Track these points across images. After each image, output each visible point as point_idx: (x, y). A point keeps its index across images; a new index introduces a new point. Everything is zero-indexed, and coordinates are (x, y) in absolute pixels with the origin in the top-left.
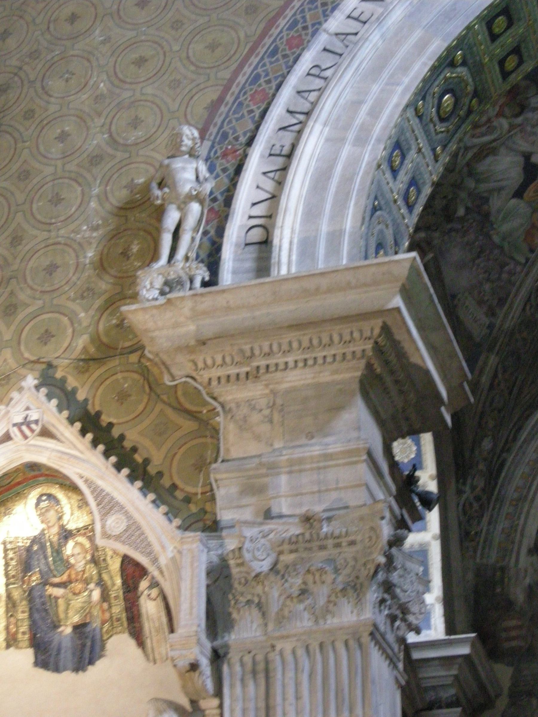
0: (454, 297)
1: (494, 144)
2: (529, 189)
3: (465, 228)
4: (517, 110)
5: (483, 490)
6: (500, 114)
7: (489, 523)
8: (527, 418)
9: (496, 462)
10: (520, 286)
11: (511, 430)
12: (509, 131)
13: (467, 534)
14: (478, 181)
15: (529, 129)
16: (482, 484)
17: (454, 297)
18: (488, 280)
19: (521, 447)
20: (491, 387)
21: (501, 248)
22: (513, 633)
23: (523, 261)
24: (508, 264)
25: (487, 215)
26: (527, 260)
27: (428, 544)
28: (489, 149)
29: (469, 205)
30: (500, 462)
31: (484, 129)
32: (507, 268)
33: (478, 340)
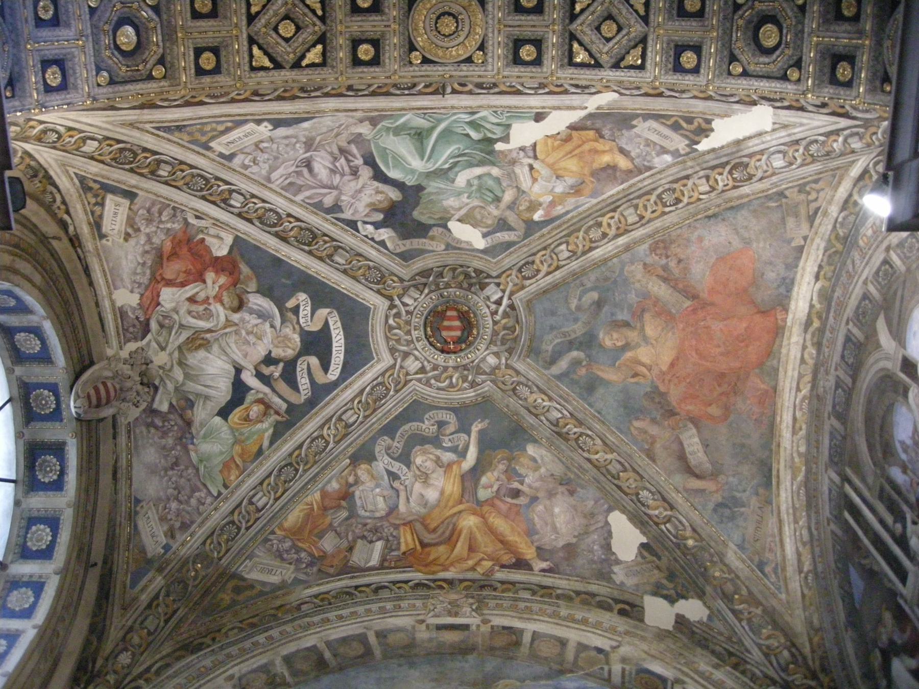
1: (208, 336)
2: (234, 412)
3: (165, 429)
4: (236, 303)
6: (218, 299)
8: (178, 659)
9: (131, 681)
10: (207, 518)
11: (156, 662)
12: (225, 328)
14: (187, 376)
15: (244, 333)
17: (138, 501)
18: (177, 499)
19: (163, 680)
20: (149, 606)
21: (197, 470)
23: (216, 494)
24: (199, 490)
25: (189, 424)
26: (220, 494)
28: (203, 339)
29: (174, 403)
31: (201, 308)
32: (197, 494)
33: (149, 555)
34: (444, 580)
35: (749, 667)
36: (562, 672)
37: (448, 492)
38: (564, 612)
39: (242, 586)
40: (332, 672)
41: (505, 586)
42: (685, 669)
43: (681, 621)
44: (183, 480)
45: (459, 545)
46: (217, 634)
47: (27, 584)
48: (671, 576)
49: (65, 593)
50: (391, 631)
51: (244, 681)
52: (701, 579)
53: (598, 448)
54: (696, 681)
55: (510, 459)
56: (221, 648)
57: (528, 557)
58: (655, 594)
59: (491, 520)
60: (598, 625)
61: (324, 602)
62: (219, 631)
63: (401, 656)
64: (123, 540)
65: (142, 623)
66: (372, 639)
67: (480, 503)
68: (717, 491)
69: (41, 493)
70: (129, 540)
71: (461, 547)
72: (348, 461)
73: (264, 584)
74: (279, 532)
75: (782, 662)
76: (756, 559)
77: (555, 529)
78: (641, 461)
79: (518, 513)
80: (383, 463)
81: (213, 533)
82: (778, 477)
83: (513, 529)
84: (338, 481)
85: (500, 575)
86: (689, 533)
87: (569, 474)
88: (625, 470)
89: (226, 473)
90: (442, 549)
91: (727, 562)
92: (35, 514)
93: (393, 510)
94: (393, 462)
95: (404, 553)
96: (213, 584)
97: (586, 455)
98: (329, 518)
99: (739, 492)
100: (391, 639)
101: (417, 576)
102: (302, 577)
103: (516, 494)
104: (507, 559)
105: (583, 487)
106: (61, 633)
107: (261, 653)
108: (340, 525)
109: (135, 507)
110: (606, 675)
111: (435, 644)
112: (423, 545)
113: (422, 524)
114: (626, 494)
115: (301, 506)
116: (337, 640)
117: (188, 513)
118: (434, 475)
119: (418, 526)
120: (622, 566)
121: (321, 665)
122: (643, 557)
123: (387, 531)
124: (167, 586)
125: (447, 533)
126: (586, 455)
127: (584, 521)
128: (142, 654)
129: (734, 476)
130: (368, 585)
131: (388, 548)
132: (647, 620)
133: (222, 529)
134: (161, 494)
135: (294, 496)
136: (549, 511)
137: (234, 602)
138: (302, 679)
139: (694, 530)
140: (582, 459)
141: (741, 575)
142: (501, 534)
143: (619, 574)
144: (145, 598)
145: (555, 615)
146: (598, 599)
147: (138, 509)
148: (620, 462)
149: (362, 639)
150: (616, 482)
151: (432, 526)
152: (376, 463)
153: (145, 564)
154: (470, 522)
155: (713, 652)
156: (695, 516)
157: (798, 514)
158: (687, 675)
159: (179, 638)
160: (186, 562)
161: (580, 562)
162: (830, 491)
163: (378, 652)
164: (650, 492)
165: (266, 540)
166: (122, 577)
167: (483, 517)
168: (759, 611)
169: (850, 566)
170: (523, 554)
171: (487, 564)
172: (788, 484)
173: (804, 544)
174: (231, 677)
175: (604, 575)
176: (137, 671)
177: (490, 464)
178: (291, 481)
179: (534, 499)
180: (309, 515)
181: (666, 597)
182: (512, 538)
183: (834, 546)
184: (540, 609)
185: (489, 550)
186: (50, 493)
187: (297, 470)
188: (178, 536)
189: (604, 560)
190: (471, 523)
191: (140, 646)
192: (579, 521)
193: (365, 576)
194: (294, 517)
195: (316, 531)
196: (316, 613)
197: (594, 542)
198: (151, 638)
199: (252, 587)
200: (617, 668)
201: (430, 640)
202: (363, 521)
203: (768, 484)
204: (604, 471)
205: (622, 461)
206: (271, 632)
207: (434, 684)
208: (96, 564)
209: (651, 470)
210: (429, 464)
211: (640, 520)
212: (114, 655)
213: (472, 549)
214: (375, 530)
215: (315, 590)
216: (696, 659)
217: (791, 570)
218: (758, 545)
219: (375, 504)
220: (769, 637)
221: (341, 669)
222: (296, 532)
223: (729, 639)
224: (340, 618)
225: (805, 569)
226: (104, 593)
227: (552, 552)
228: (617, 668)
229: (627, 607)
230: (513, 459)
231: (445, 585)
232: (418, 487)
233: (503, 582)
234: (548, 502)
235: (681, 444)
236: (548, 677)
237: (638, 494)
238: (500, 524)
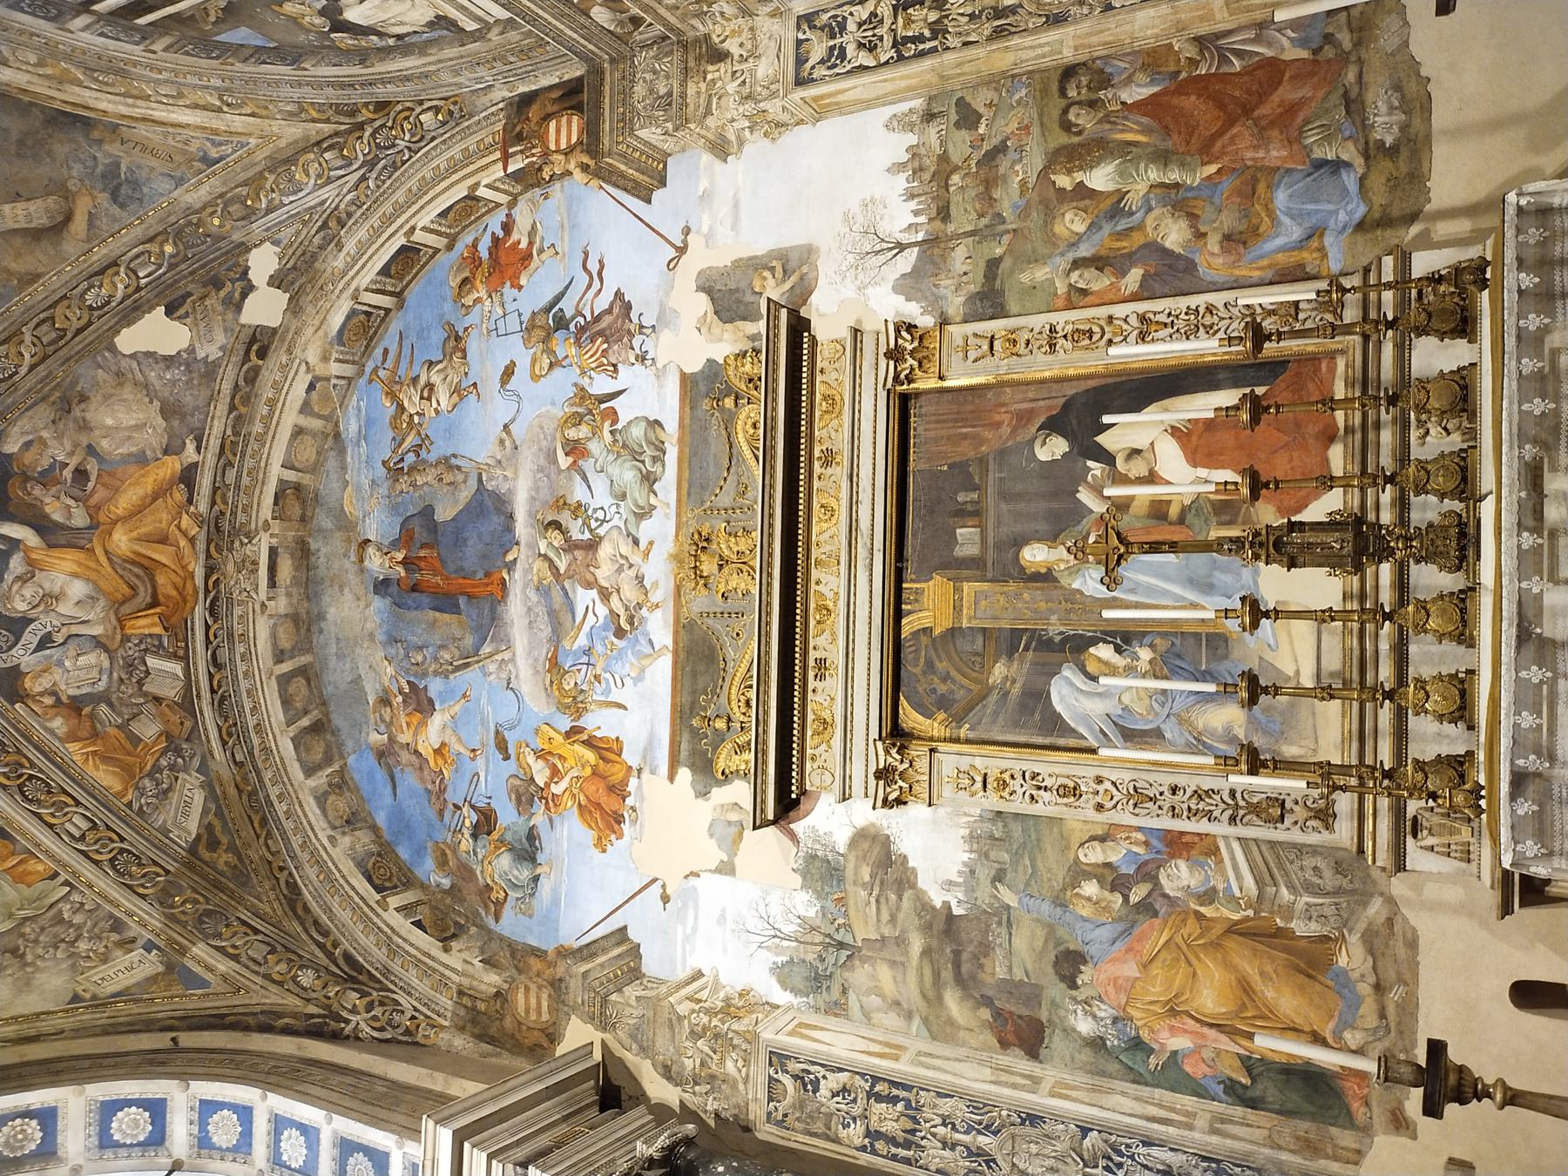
0: (76, 998)
5: (363, 995)
7: (409, 994)
8: (306, 909)
9: (338, 966)
13: (408, 1032)
16: (356, 995)
17: (76, 998)
18: (72, 943)
20: (235, 958)
21: (26, 919)
22: (533, 1001)
24: (60, 912)
26: (66, 883)
27: (335, 1132)
30: (341, 962)
32: (66, 916)
33: (161, 969)
34: (207, 578)
35: (342, 206)
36: (337, 436)
37: (75, 568)
38: (258, 428)
39: (208, 838)
40: (327, 714)
41: (218, 500)
42: (340, 286)
43: (277, 281)
44: (42, 938)
45: (156, 556)
46: (275, 865)
47: (203, 1124)
48: (218, 284)
49: (217, 1071)
50: (275, 645)
51: (337, 823)
52: (222, 244)
53: (13, 351)
54: (358, 273)
55: (26, 478)
56: (294, 857)
57: (178, 467)
58: (239, 308)
59: (120, 512)
60: (277, 386)
61: (232, 732)
62: (270, 863)
63: (309, 630)
64: (135, 1009)
65: (259, 964)
66: (286, 667)
67: (94, 526)
68: (94, 198)
69: (60, 1139)
70: (136, 1001)
71: (161, 555)
72: (17, 706)
73: (205, 812)
74: (130, 797)
75: (340, 163)
76: (197, 164)
77: (139, 427)
78: (38, 293)
79: (111, 474)
80: (23, 656)
81: (130, 887)
82: (73, 104)
83: (137, 483)
84: (52, 719)
85: (202, 506)
86: (154, 247)
87: (52, 399)
88: (52, 319)
89: (33, 878)
90: (161, 580)
91: (198, 206)
92: (95, 1141)
93: (98, 643)
94: (23, 641)
95: (166, 629)
96: (205, 877)
97: (23, 370)
98: (109, 730)
99: (96, 166)
100: (286, 644)
101: (200, 613)
102: (196, 762)
103: (81, 474)
104: (179, 495)
105: (75, 383)
106: (272, 1063)
107: (301, 806)
108: (120, 714)
109: (84, 1000)
110: (343, 382)
111: (294, 591)
112: (155, 603)
113: (123, 603)
114: (90, 323)
115: (90, 769)
116: (285, 712)
117: (95, 925)
118: (47, 586)
119: (126, 609)
120: (197, 345)
121: (317, 728)
122: (187, 315)
123: (131, 650)
124: (206, 937)
125: (136, 570)
126: (23, 370)
127: (128, 388)
128: (301, 957)
129: (70, 168)
130: (211, 676)
131: (159, 650)
132: (275, 324)
133: (122, 875)
134: (64, 966)
135: (73, 780)
136: (109, 432)
137: (232, 848)
138: (335, 750)
139: (150, 240)
140: (30, 377)
141: (220, 190)
142: (143, 499)
143: (209, 351)
144: (223, 966)
145: (261, 439)
146: (241, 383)
147: (88, 996)
148: (38, 325)
149: (284, 681)
150: (69, 335)
151: (127, 590)
152: (22, 667)
153: (175, 971)
154: (122, 541)
155: (321, 248)
156: (128, 236)
157: (135, 92)
158: (348, 284)
159: (280, 912)
160: (172, 918)
161: (188, 399)
162: (102, 35)
163: (304, 660)
164: (88, 289)
165: (141, 812)
166: (194, 1002)
167: (115, 523)
168: (271, 178)
169: (217, 38)
170: (173, 475)
171: (186, 521)
172: (87, 93)
173: (180, 95)
174: (331, 839)
175: (210, 371)
176: (324, 961)
177: (34, 506)
178: (48, 785)
179: (91, 450)
180: (106, 759)
181: (244, 295)
182: (148, 485)
183: (187, 53)
184: (252, 457)
185: (165, 516)
186: (60, 1125)
187: (31, 777)
188: (131, 934)
189: (188, 365)
190: (124, 538)
191: (291, 960)
192: (127, 392)
193: (197, 682)
194: (106, 777)
195: (128, 746)
196: (247, 740)
197: (160, 378)
198: (279, 948)
199: (210, 827)
200: (335, 368)
201: (289, 595)
202: (115, 685)
203: (87, 123)
204: (52, 348)
205: (36, 320)
206: (273, 798)
207: (346, 590)
208: (173, 1039)
209: (53, 283)
210: (28, 591)
211: (132, 311)
212: (303, 993)
213: (163, 540)
214: (130, 666)
215: (215, 744)
216: (329, 270)
217: (215, 124)
218: (177, 158)
219: (90, 667)
220: (308, 175)
221: (324, 704)
222: (129, 774)
223: (305, 223)
224: (254, 709)
225: (218, 103)
226: (217, 1022)
227: (172, 434)
228: (335, 368)
229: (255, 348)
230: (24, 473)
231: (214, 577)
232: (65, 608)
233: (213, 503)
234: (97, 433)
235: (15, 231)
236: (342, 451)
237: (91, 308)
238: (127, 500)
